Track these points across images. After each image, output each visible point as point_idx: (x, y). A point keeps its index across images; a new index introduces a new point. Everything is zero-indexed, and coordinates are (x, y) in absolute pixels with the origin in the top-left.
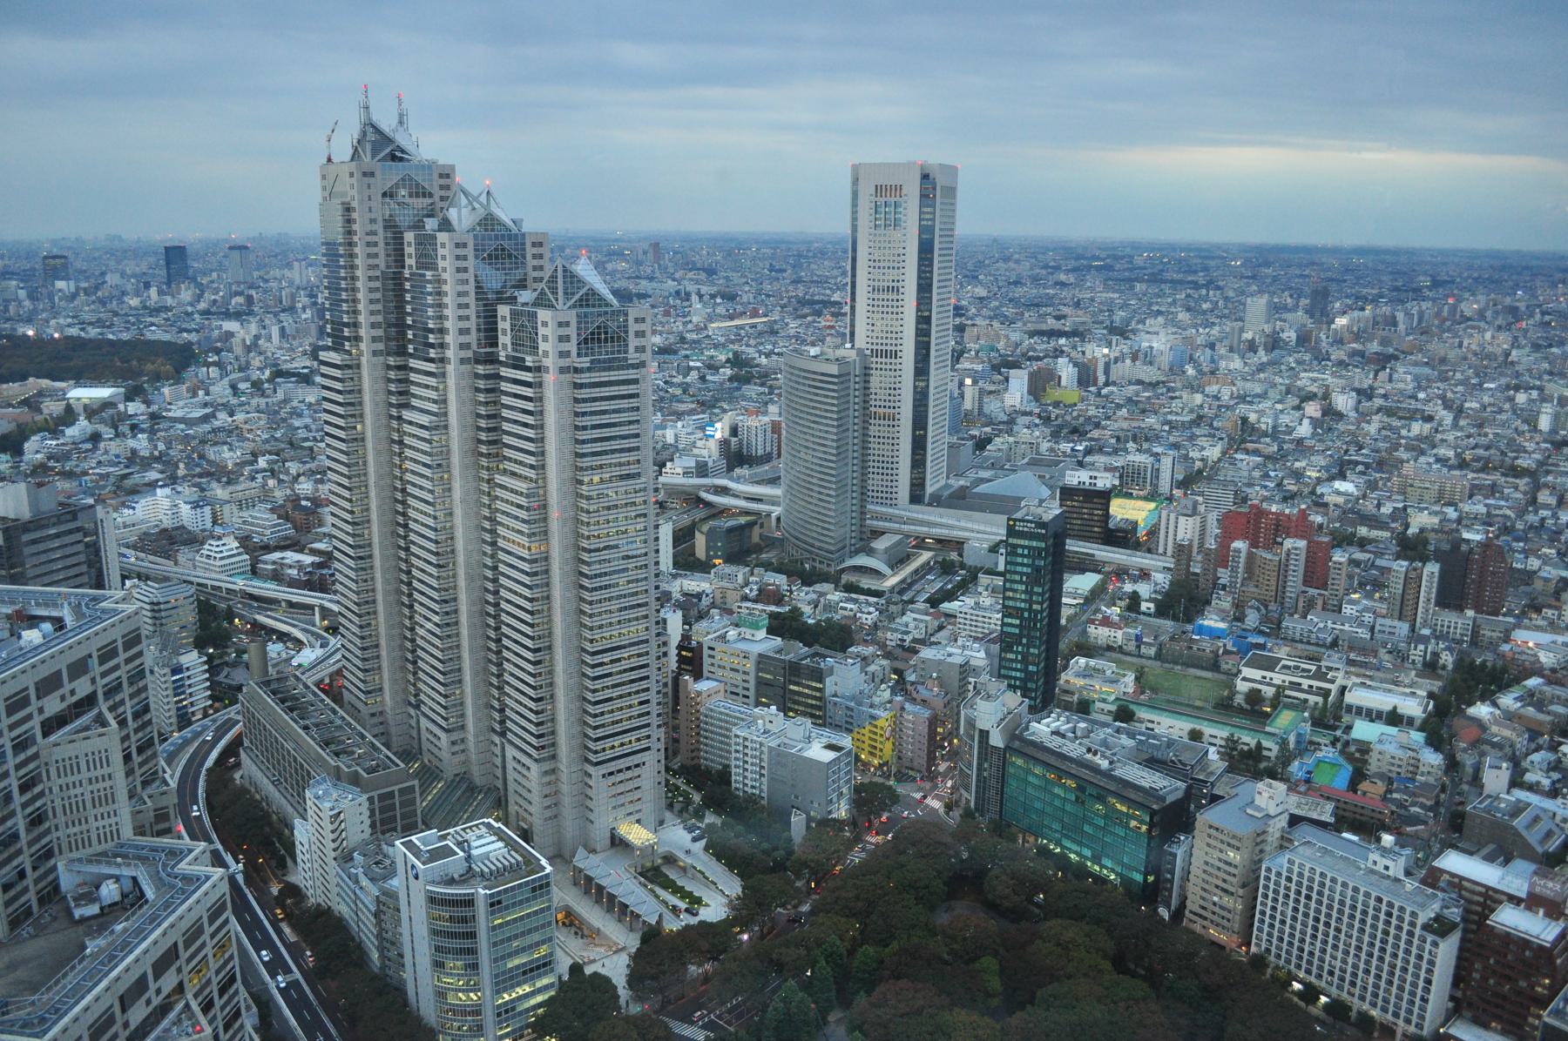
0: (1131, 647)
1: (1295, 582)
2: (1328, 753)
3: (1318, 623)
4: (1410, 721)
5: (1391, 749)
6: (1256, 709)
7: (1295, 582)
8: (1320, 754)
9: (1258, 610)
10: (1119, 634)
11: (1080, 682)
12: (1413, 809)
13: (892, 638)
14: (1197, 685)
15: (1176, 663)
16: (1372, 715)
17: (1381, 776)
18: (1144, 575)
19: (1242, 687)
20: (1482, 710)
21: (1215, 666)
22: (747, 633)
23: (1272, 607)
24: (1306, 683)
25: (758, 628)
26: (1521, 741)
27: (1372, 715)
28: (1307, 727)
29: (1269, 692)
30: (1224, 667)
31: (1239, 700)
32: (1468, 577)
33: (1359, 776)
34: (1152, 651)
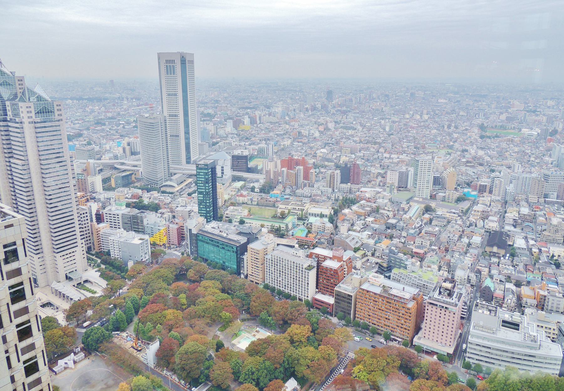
0: (249, 202)
1: (301, 179)
2: (302, 227)
3: (307, 191)
4: (326, 216)
5: (318, 224)
6: (283, 216)
7: (301, 179)
8: (299, 228)
9: (290, 188)
10: (246, 199)
11: (230, 213)
12: (322, 240)
13: (173, 205)
14: (268, 212)
15: (263, 206)
16: (315, 215)
17: (315, 232)
18: (257, 181)
19: (279, 211)
20: (346, 211)
21: (274, 206)
22: (119, 207)
23: (294, 187)
24: (297, 208)
25: (122, 206)
26: (355, 218)
27: (315, 215)
28: (296, 221)
29: (287, 211)
30: (276, 205)
31: (279, 215)
32: (349, 174)
33: (309, 232)
34: (256, 203)
